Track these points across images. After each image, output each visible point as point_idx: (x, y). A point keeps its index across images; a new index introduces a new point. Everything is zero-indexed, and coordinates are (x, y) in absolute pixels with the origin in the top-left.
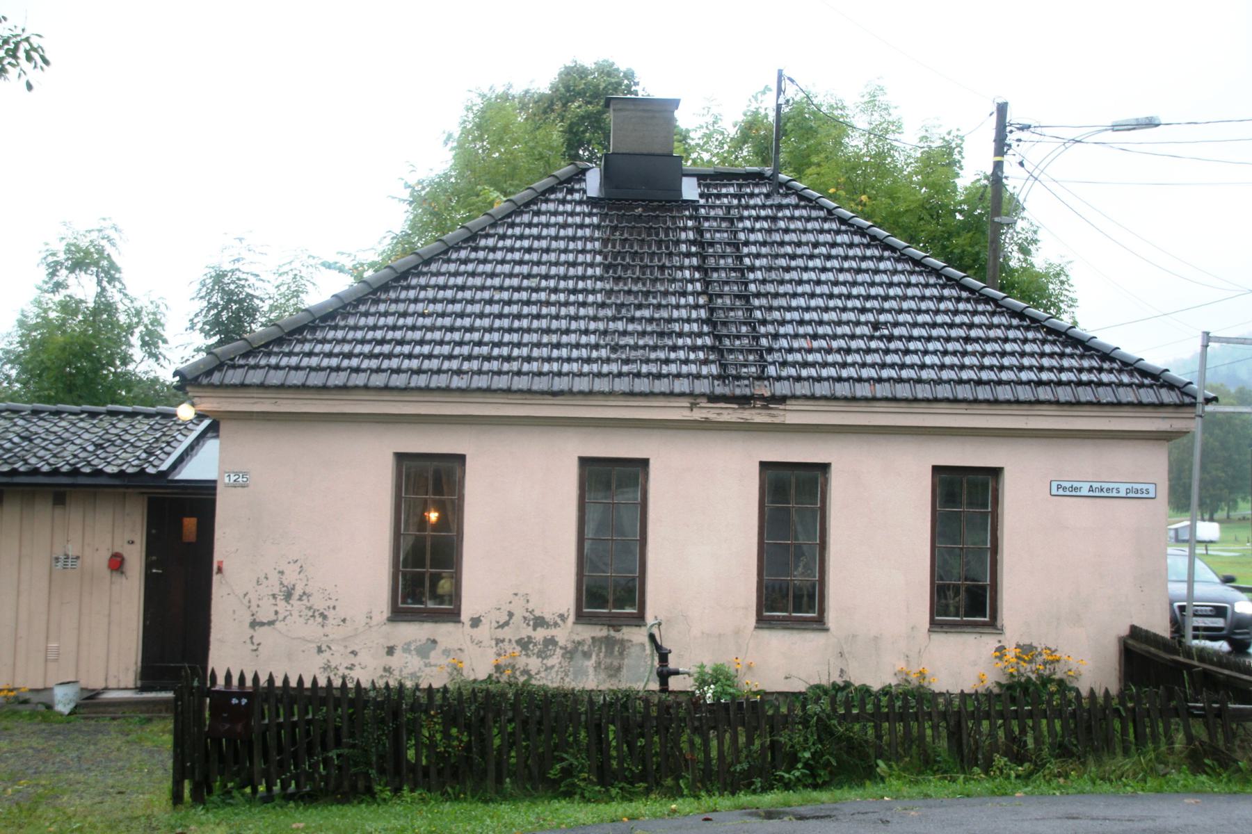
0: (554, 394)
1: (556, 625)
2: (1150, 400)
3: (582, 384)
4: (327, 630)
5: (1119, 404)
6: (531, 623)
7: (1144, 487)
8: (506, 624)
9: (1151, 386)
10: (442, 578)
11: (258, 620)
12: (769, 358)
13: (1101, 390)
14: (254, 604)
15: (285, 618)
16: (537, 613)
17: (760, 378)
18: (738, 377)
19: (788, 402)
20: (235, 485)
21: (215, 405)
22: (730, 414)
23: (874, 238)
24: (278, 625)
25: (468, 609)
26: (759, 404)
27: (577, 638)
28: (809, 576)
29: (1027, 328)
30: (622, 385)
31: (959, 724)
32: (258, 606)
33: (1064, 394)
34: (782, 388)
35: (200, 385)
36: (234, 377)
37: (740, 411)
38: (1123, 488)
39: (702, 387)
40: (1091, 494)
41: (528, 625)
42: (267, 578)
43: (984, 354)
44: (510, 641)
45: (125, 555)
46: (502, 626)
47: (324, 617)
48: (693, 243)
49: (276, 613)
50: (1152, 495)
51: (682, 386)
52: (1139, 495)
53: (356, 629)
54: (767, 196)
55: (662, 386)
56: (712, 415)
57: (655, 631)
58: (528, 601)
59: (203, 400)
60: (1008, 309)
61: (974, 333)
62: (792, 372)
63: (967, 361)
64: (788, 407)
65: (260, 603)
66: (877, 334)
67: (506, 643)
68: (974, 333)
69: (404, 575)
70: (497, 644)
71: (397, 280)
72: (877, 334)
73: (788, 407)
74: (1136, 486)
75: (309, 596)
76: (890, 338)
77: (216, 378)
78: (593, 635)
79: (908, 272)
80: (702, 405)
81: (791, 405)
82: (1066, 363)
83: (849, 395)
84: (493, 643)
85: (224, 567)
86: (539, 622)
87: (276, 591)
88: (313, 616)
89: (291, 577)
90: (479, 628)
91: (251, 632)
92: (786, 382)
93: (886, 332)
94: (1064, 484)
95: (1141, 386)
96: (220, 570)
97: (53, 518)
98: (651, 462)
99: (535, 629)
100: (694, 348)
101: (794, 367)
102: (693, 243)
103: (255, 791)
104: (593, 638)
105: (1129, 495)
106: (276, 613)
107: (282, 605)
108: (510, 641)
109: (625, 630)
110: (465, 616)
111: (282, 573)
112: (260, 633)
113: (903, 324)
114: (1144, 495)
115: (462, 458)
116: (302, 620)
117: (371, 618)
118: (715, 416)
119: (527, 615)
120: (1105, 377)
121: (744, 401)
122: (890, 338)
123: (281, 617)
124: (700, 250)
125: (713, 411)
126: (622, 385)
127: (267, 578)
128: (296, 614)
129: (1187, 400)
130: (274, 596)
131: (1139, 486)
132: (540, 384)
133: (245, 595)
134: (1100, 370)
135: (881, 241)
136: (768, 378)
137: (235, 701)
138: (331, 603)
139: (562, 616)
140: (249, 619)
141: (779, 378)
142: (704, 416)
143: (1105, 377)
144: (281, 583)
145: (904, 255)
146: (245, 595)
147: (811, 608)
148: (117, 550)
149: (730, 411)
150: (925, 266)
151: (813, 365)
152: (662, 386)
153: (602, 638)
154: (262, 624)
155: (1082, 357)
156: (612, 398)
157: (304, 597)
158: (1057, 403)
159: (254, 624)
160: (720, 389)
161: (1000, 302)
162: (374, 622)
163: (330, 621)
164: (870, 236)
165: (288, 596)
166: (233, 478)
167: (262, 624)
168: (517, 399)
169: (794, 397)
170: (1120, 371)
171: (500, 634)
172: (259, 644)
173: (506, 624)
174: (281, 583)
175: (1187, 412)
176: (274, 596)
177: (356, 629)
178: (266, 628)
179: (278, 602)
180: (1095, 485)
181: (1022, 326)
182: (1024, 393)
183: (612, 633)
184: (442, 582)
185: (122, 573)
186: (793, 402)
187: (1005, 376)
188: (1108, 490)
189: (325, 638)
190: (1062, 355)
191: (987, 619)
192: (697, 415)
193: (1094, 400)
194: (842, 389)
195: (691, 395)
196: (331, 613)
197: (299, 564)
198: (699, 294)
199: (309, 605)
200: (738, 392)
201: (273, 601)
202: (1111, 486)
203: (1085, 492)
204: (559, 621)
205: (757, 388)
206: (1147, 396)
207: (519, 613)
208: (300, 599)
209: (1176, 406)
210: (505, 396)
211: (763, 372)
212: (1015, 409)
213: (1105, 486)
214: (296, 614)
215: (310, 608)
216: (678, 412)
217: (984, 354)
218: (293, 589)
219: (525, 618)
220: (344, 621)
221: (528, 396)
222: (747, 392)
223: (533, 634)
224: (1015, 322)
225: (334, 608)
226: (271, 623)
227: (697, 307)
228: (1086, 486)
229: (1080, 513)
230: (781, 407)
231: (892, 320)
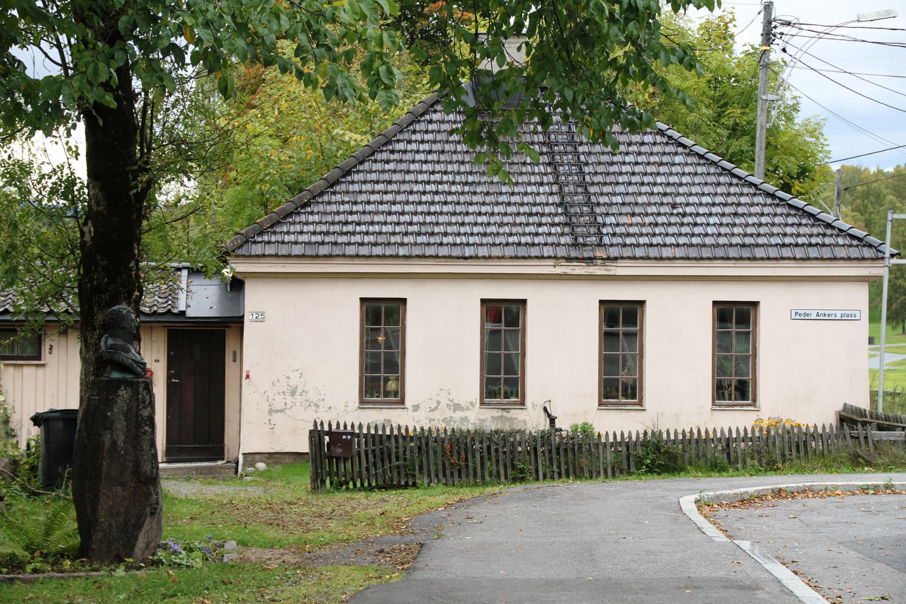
1: (468, 409)
2: (856, 256)
3: (483, 251)
5: (835, 259)
6: (452, 408)
7: (853, 313)
8: (436, 408)
9: (857, 246)
10: (389, 380)
11: (273, 409)
12: (604, 231)
13: (824, 249)
17: (599, 245)
18: (585, 245)
23: (670, 137)
25: (409, 401)
26: (599, 261)
27: (482, 417)
28: (631, 375)
29: (777, 205)
30: (509, 251)
31: (728, 445)
33: (799, 253)
34: (614, 252)
37: (587, 267)
39: (562, 252)
40: (818, 318)
41: (450, 409)
42: (278, 381)
43: (747, 225)
44: (438, 420)
45: (153, 370)
46: (432, 410)
47: (318, 406)
48: (544, 144)
49: (286, 404)
50: (858, 318)
51: (548, 251)
52: (849, 318)
53: (338, 414)
55: (534, 251)
57: (547, 405)
60: (764, 191)
61: (741, 210)
62: (619, 240)
63: (736, 230)
64: (618, 265)
65: (275, 397)
66: (675, 211)
67: (436, 421)
68: (741, 210)
69: (366, 377)
70: (430, 422)
72: (675, 211)
73: (618, 265)
74: (847, 312)
76: (684, 215)
77: (239, 252)
79: (695, 164)
81: (621, 263)
82: (802, 230)
83: (658, 256)
84: (428, 421)
86: (457, 407)
89: (294, 381)
92: (616, 248)
93: (681, 210)
94: (800, 312)
95: (851, 246)
96: (248, 377)
97: (59, 344)
99: (454, 412)
100: (553, 225)
101: (621, 237)
102: (544, 144)
103: (355, 484)
104: (492, 417)
105: (843, 318)
106: (286, 404)
107: (289, 399)
108: (438, 420)
109: (512, 411)
111: (288, 378)
112: (276, 418)
113: (693, 204)
114: (853, 318)
115: (404, 301)
116: (303, 408)
119: (449, 403)
120: (827, 241)
121: (590, 260)
122: (684, 215)
123: (288, 406)
124: (549, 150)
126: (509, 251)
127: (278, 381)
128: (298, 404)
129: (880, 255)
131: (849, 313)
134: (824, 235)
135: (676, 140)
136: (605, 245)
137: (344, 437)
138: (322, 397)
139: (472, 403)
140: (267, 408)
141: (612, 245)
143: (827, 241)
144: (288, 385)
145: (692, 151)
147: (633, 396)
149: (580, 267)
150: (707, 159)
151: (633, 235)
152: (534, 251)
154: (278, 411)
155: (813, 225)
156: (503, 260)
157: (304, 394)
158: (795, 259)
159: (271, 412)
160: (573, 254)
161: (759, 187)
162: (349, 409)
163: (321, 409)
164: (667, 136)
165: (293, 393)
166: (255, 316)
167: (278, 411)
169: (623, 258)
170: (838, 236)
171: (432, 415)
172: (275, 425)
173: (436, 408)
174: (288, 385)
175: (880, 263)
177: (338, 414)
179: (287, 397)
181: (774, 204)
182: (773, 252)
183: (505, 414)
184: (390, 383)
186: (622, 261)
187: (761, 240)
188: (829, 315)
190: (800, 225)
191: (750, 402)
192: (559, 270)
193: (819, 257)
194: (653, 252)
195: (556, 258)
196: (321, 404)
197: (299, 372)
198: (552, 184)
199: (307, 398)
200: (586, 255)
201: (283, 396)
202: (830, 312)
204: (470, 407)
205: (598, 252)
206: (854, 253)
207: (444, 402)
208: (301, 395)
209: (872, 259)
210: (434, 260)
211: (601, 240)
213: (827, 312)
214: (298, 404)
215: (308, 400)
217: (747, 225)
218: (296, 388)
220: (330, 408)
221: (449, 260)
222: (591, 255)
223: (453, 415)
224: (769, 201)
225: (323, 400)
226: (281, 411)
227: (551, 194)
231: (685, 202)
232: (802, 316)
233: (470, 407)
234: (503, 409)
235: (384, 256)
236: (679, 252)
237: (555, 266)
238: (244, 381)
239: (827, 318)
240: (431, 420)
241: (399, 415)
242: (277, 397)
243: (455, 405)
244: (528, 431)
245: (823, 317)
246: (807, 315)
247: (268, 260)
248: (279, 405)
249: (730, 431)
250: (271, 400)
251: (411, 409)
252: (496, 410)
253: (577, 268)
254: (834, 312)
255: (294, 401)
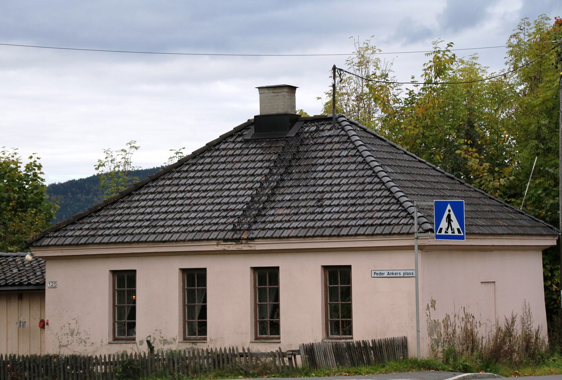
0: (165, 242)
1: (172, 343)
4: (86, 348)
6: (162, 342)
7: (411, 272)
14: (60, 338)
15: (71, 343)
16: (165, 338)
19: (255, 240)
21: (41, 254)
22: (233, 247)
24: (69, 346)
26: (244, 241)
30: (190, 236)
35: (33, 246)
37: (237, 245)
38: (402, 272)
40: (389, 276)
41: (161, 343)
47: (86, 342)
49: (68, 341)
50: (414, 275)
52: (409, 276)
53: (97, 347)
56: (226, 248)
58: (161, 333)
64: (256, 243)
74: (407, 271)
75: (80, 333)
81: (257, 242)
85: (49, 323)
87: (68, 332)
88: (81, 342)
89: (73, 326)
94: (377, 272)
96: (47, 324)
98: (207, 269)
99: (164, 345)
105: (405, 276)
106: (68, 341)
107: (70, 337)
109: (198, 344)
110: (137, 340)
111: (70, 324)
116: (77, 344)
117: (102, 342)
118: (227, 248)
121: (238, 241)
125: (226, 246)
127: (64, 327)
128: (75, 341)
133: (57, 334)
138: (88, 336)
139: (174, 339)
144: (70, 329)
146: (57, 334)
149: (233, 245)
154: (64, 346)
157: (78, 334)
162: (104, 344)
163: (88, 344)
165: (72, 334)
166: (51, 284)
167: (64, 346)
174: (70, 329)
176: (67, 334)
180: (390, 272)
183: (194, 346)
188: (396, 273)
189: (86, 352)
192: (220, 248)
196: (88, 341)
197: (76, 320)
199: (80, 337)
201: (66, 336)
202: (397, 272)
203: (386, 275)
204: (173, 342)
208: (76, 335)
212: (349, 239)
213: (394, 272)
214: (75, 341)
215: (80, 339)
218: (74, 331)
219: (160, 340)
220: (93, 343)
223: (163, 347)
225: (89, 338)
226: (66, 346)
228: (386, 273)
229: (384, 284)
230: (253, 243)
232: (379, 275)
233: (173, 342)
234: (193, 343)
236: (294, 233)
237: (217, 245)
239: (395, 276)
242: (64, 337)
243: (165, 340)
244: (94, 357)
245: (392, 276)
247: (53, 248)
248: (64, 342)
250: (60, 339)
251: (138, 343)
252: (188, 343)
253: (231, 246)
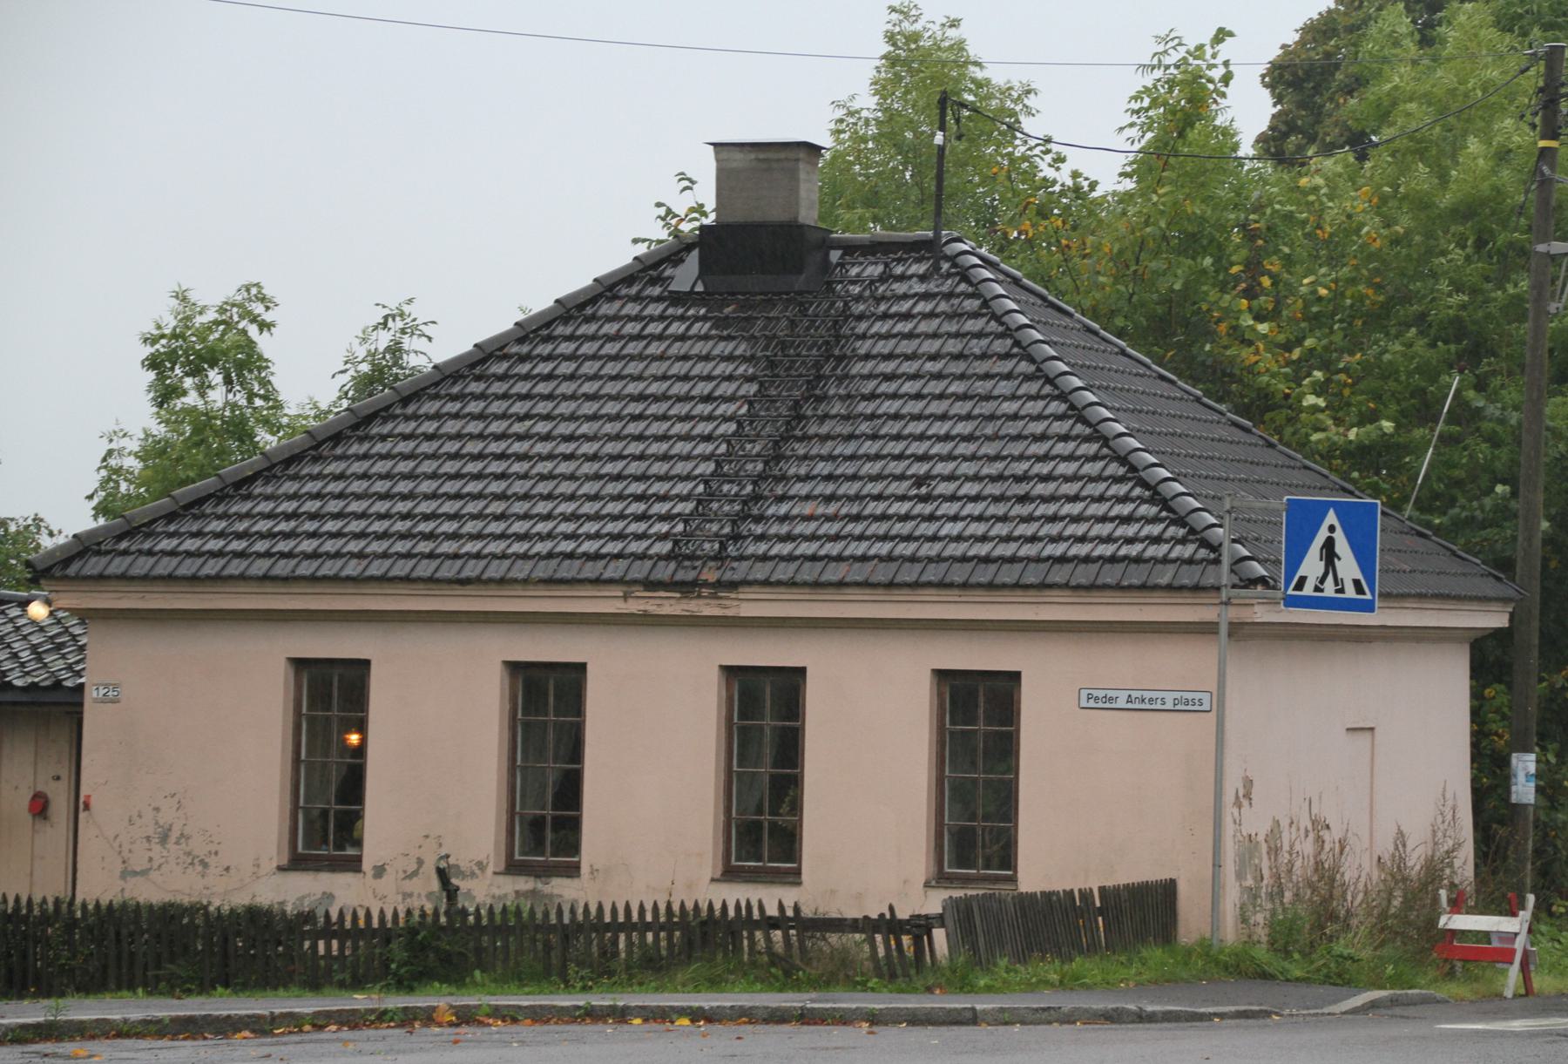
1: (473, 874)
7: (1197, 696)
8: (415, 874)
14: (125, 848)
15: (160, 866)
19: (741, 590)
20: (105, 700)
21: (74, 602)
22: (671, 606)
24: (154, 875)
26: (705, 592)
32: (130, 851)
35: (53, 578)
36: (94, 565)
38: (1169, 697)
40: (1130, 706)
45: (50, 795)
47: (205, 864)
49: (151, 859)
50: (1206, 707)
54: (923, 278)
56: (651, 607)
58: (440, 845)
59: (61, 595)
67: (415, 898)
70: (404, 899)
71: (355, 427)
78: (517, 888)
80: (638, 594)
81: (746, 593)
84: (400, 898)
85: (93, 802)
87: (150, 832)
88: (192, 864)
89: (166, 817)
90: (383, 879)
91: (122, 882)
94: (1095, 693)
96: (87, 807)
98: (589, 667)
104: (517, 892)
105: (1177, 707)
106: (151, 859)
108: (419, 895)
110: (367, 865)
111: (157, 809)
117: (258, 866)
125: (652, 601)
127: (140, 816)
130: (148, 839)
131: (1189, 696)
132: (448, 570)
135: (1024, 349)
138: (213, 848)
140: (119, 867)
142: (642, 608)
144: (157, 823)
148: (40, 788)
149: (672, 602)
153: (527, 892)
154: (135, 873)
163: (212, 870)
165: (164, 839)
166: (102, 692)
167: (135, 873)
168: (420, 588)
171: (409, 886)
173: (415, 874)
174: (157, 823)
176: (148, 839)
178: (139, 879)
180: (1134, 694)
183: (540, 886)
185: (45, 818)
186: (747, 590)
188: (1151, 700)
189: (205, 892)
192: (633, 607)
196: (212, 861)
197: (176, 799)
199: (188, 849)
201: (147, 846)
202: (1154, 695)
203: (1121, 703)
204: (477, 872)
208: (177, 843)
212: (1018, 596)
213: (1147, 695)
215: (189, 854)
216: (609, 603)
218: (170, 830)
220: (227, 869)
225: (216, 853)
226: (144, 873)
228: (1123, 695)
230: (733, 596)
233: (477, 872)
235: (313, 579)
238: (82, 815)
239: (1148, 706)
240: (407, 895)
241: (349, 885)
245: (1141, 706)
246: (1111, 699)
248: (139, 863)
249: (600, 908)
250: (126, 854)
254: (1160, 695)
255: (165, 854)
